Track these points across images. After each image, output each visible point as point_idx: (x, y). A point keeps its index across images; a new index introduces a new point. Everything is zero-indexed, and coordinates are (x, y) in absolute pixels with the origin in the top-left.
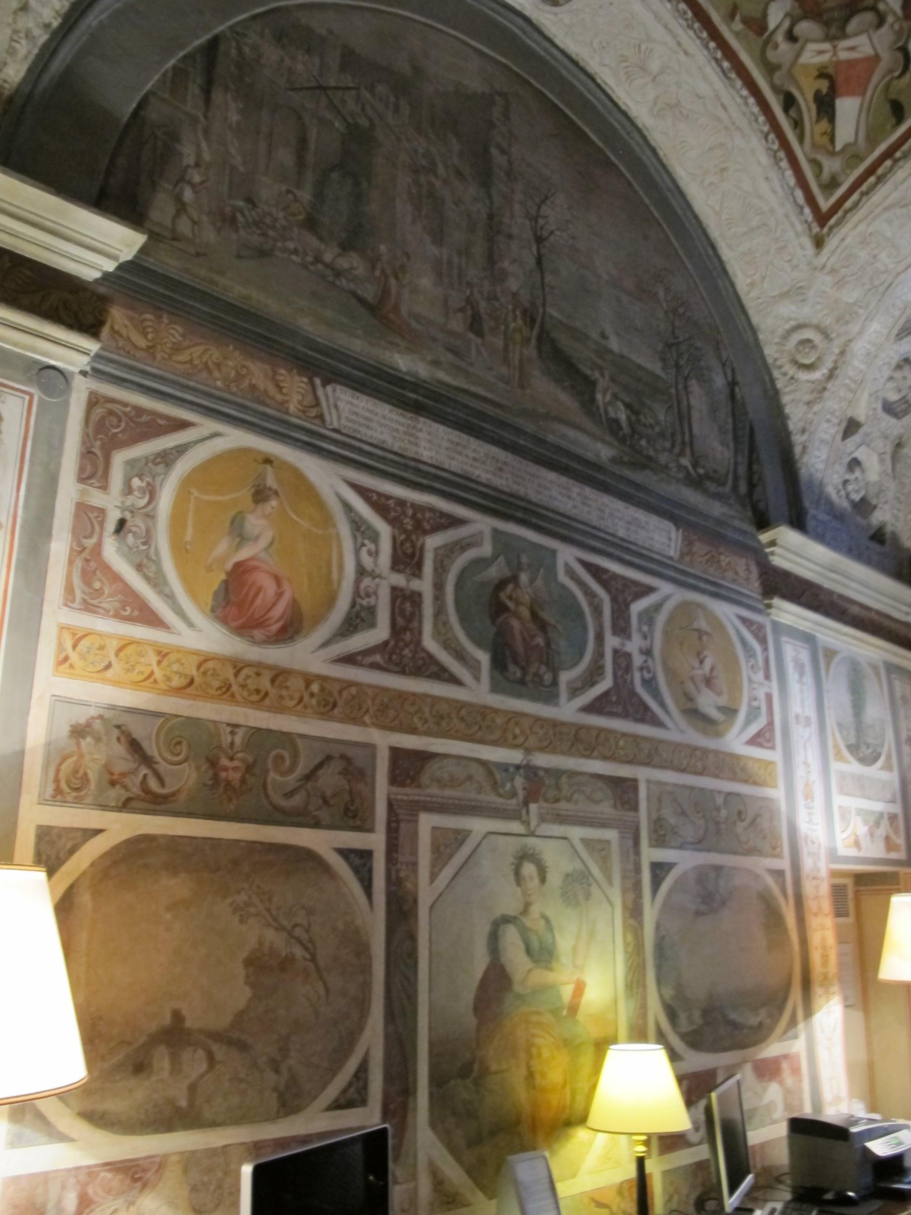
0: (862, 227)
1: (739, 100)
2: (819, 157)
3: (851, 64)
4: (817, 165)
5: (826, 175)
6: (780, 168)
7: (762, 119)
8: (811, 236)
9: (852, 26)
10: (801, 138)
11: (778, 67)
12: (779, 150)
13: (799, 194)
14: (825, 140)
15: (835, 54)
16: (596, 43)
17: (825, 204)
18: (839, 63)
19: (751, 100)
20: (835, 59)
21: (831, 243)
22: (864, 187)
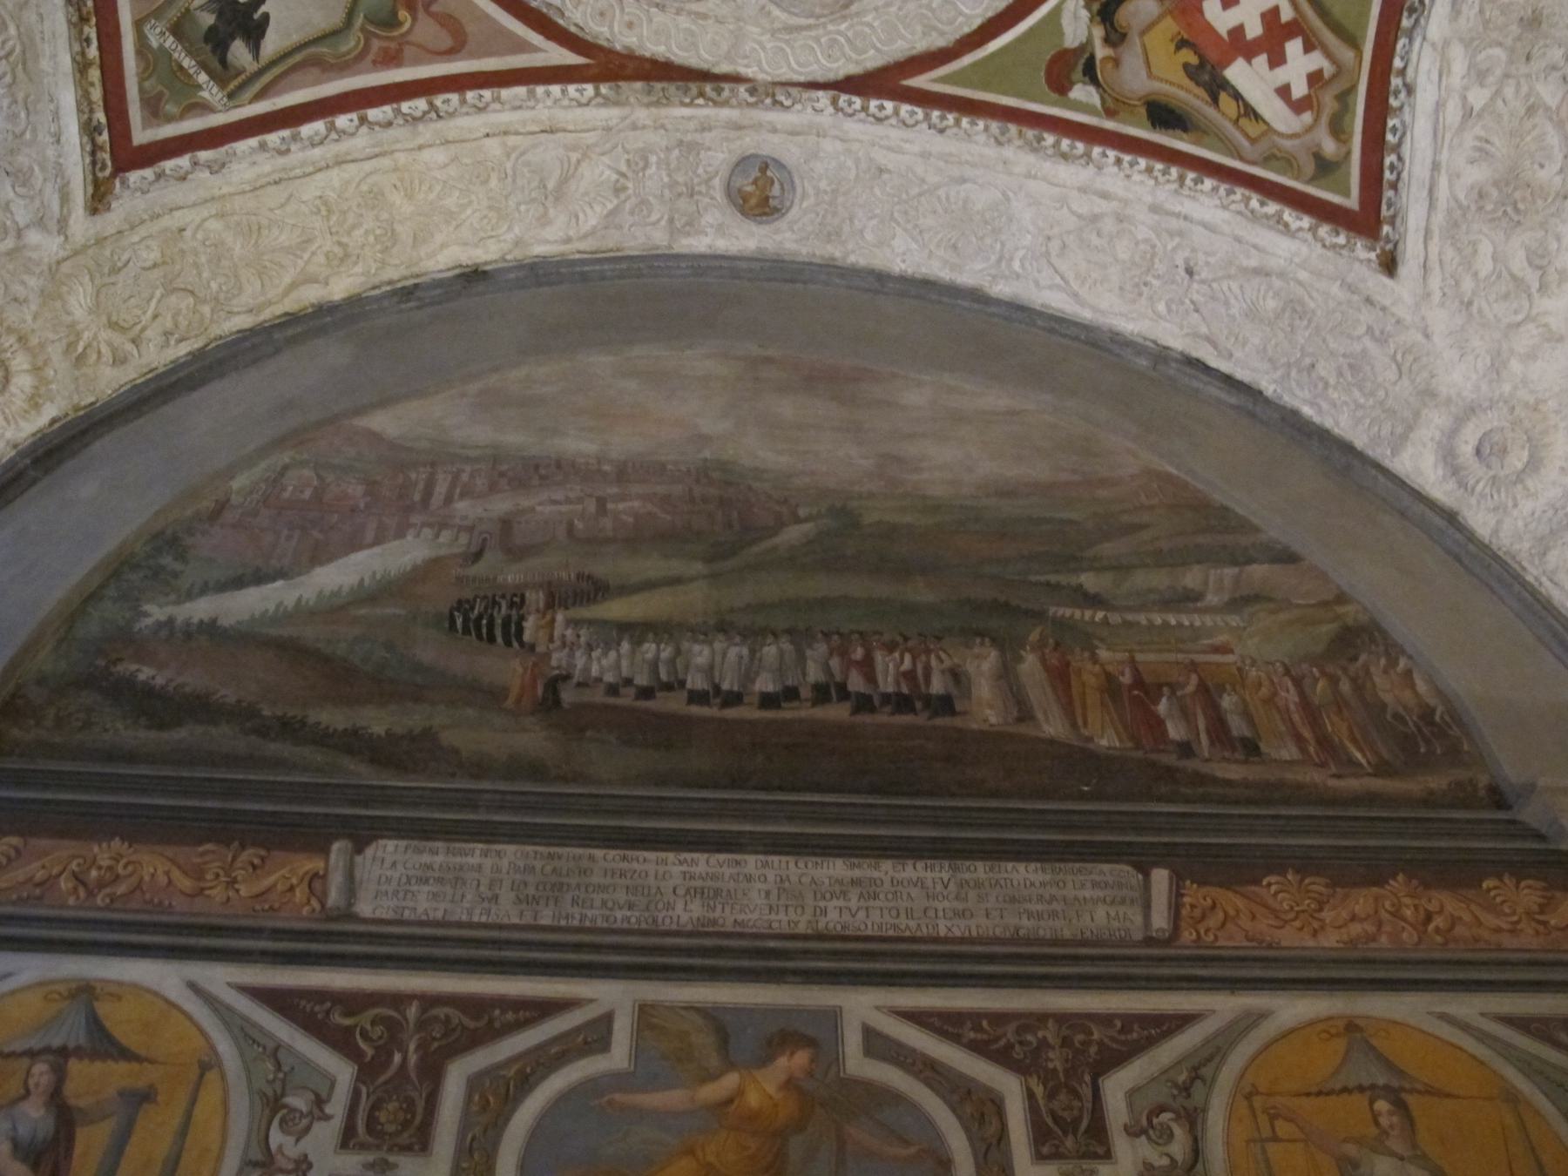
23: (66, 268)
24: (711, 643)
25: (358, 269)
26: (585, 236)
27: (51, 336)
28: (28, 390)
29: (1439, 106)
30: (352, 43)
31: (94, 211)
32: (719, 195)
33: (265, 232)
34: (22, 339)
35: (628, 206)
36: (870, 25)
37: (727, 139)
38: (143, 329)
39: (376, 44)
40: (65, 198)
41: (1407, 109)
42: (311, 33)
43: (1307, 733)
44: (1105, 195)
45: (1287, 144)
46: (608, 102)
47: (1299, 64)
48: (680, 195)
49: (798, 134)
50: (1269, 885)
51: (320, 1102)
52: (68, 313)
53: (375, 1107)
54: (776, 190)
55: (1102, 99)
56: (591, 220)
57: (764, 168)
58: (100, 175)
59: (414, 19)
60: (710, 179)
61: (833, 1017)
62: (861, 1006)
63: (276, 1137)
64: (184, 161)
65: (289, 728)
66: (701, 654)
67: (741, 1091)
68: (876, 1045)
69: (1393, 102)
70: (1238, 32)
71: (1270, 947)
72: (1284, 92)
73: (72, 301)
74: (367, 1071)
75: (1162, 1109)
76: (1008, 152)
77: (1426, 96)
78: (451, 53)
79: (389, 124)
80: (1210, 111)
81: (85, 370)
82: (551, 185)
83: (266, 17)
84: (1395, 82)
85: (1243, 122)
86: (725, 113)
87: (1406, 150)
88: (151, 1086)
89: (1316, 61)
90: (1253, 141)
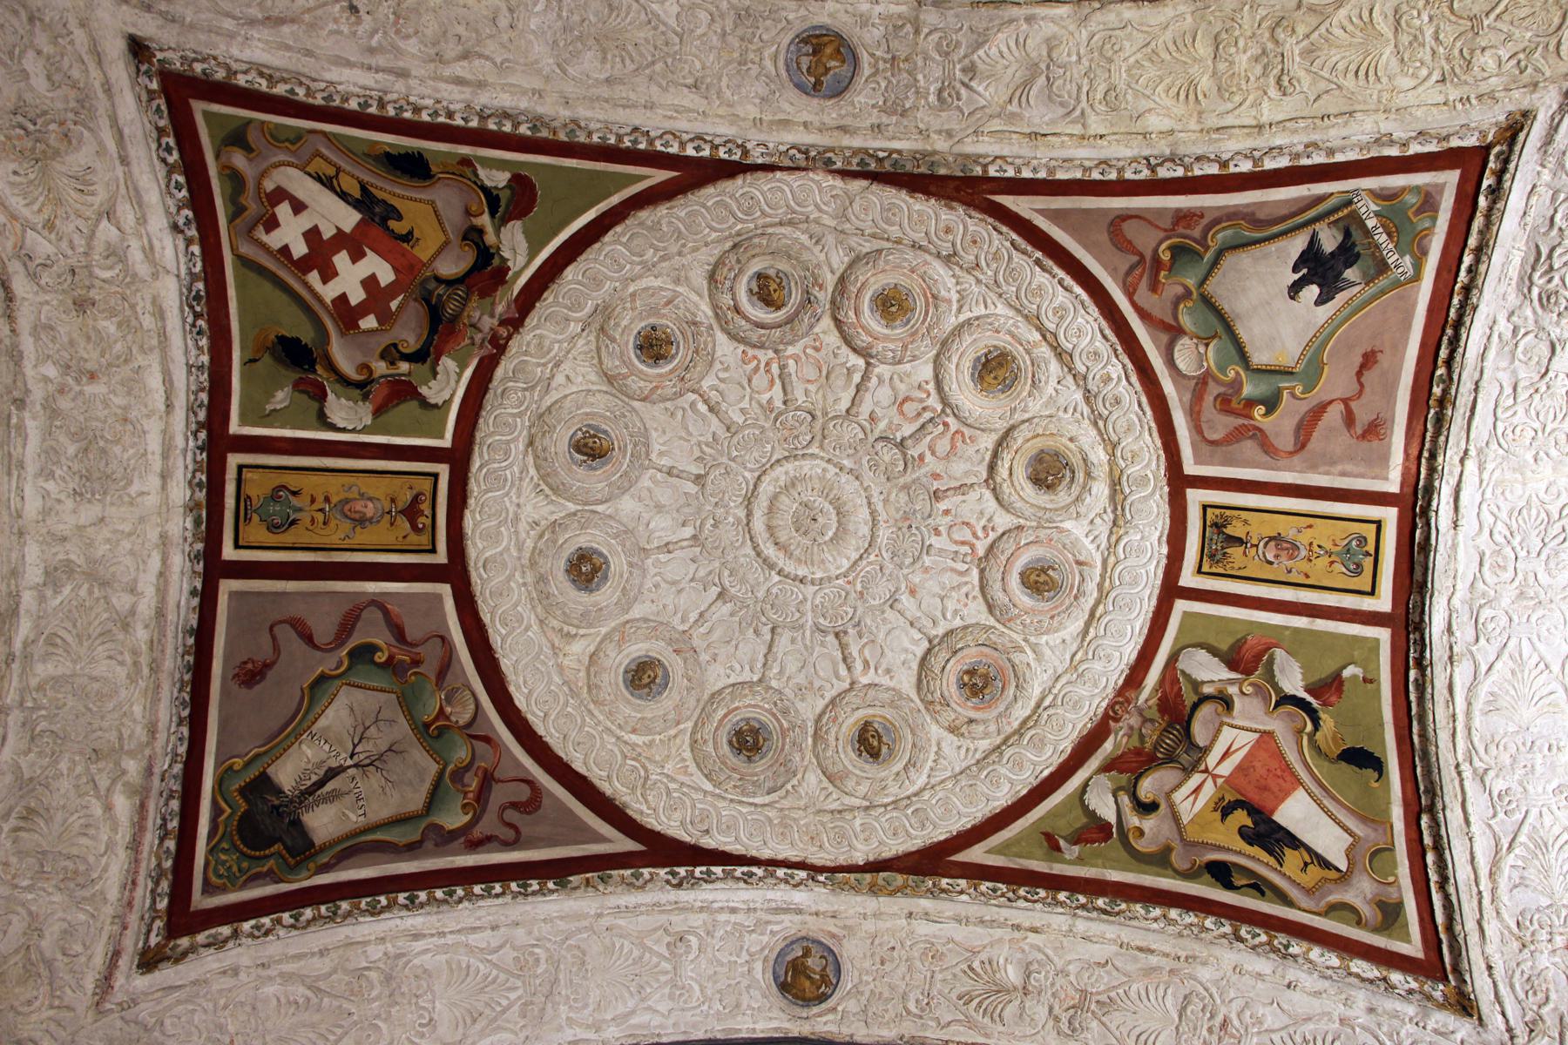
0: (1492, 928)
1: (1155, 925)
2: (1334, 898)
3: (1240, 768)
4: (1334, 909)
5: (1367, 911)
6: (1294, 957)
7: (1209, 922)
8: (1441, 1006)
9: (1200, 733)
10: (1285, 900)
11: (1168, 850)
12: (1271, 938)
13: (1359, 966)
14: (1315, 871)
15: (1215, 777)
16: (912, 1006)
17: (1413, 947)
18: (1229, 780)
19: (1174, 913)
20: (1220, 781)
21: (1481, 986)
22: (1434, 877)
26: (1011, 21)
29: (142, 220)
30: (1220, 236)
31: (1525, 114)
32: (865, 59)
33: (1353, 67)
35: (962, 52)
36: (713, 229)
37: (855, 116)
39: (1196, 233)
41: (173, 209)
42: (1256, 251)
44: (459, 81)
45: (282, 157)
46: (976, 158)
47: (290, 233)
48: (906, 60)
49: (781, 122)
54: (805, 62)
55: (477, 175)
56: (1001, 41)
57: (817, 86)
59: (1156, 251)
60: (874, 75)
64: (1415, 149)
69: (188, 213)
70: (357, 256)
72: (298, 207)
76: (565, 114)
77: (158, 223)
78: (1125, 217)
79: (1198, 159)
80: (366, 178)
82: (1042, 80)
83: (1295, 269)
84: (193, 232)
85: (331, 171)
86: (857, 143)
87: (161, 172)
89: (274, 240)
90: (319, 154)
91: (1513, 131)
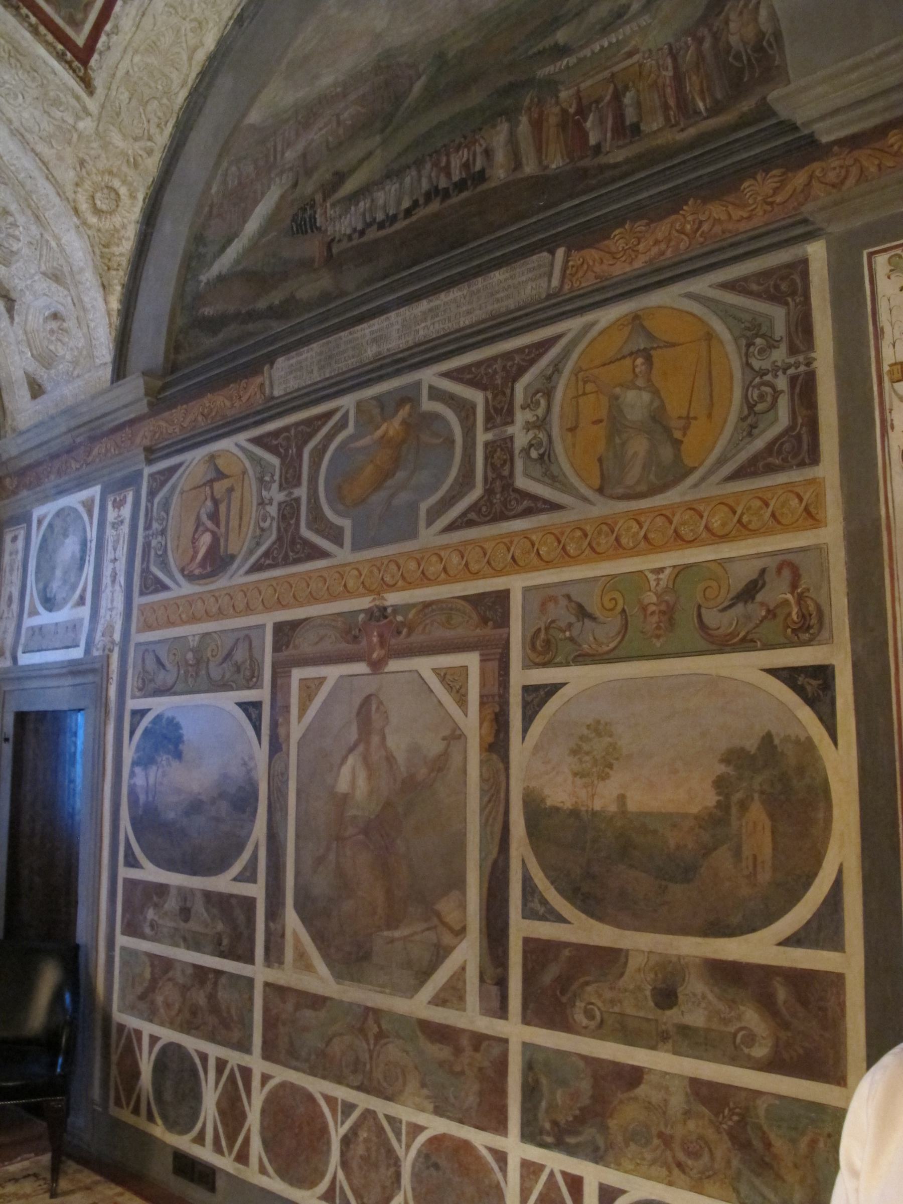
23: (101, 129)
24: (383, 189)
25: (211, 25)
27: (119, 162)
28: (127, 193)
34: (111, 173)
38: (148, 131)
40: (78, 98)
43: (672, 102)
50: (615, 236)
51: (272, 476)
52: (117, 148)
53: (287, 473)
58: (81, 74)
61: (418, 384)
62: (429, 376)
63: (264, 493)
65: (252, 316)
66: (380, 197)
67: (386, 432)
68: (436, 394)
71: (607, 279)
73: (114, 141)
74: (283, 458)
75: (538, 392)
81: (142, 167)
88: (232, 486)
91: (87, 83)
